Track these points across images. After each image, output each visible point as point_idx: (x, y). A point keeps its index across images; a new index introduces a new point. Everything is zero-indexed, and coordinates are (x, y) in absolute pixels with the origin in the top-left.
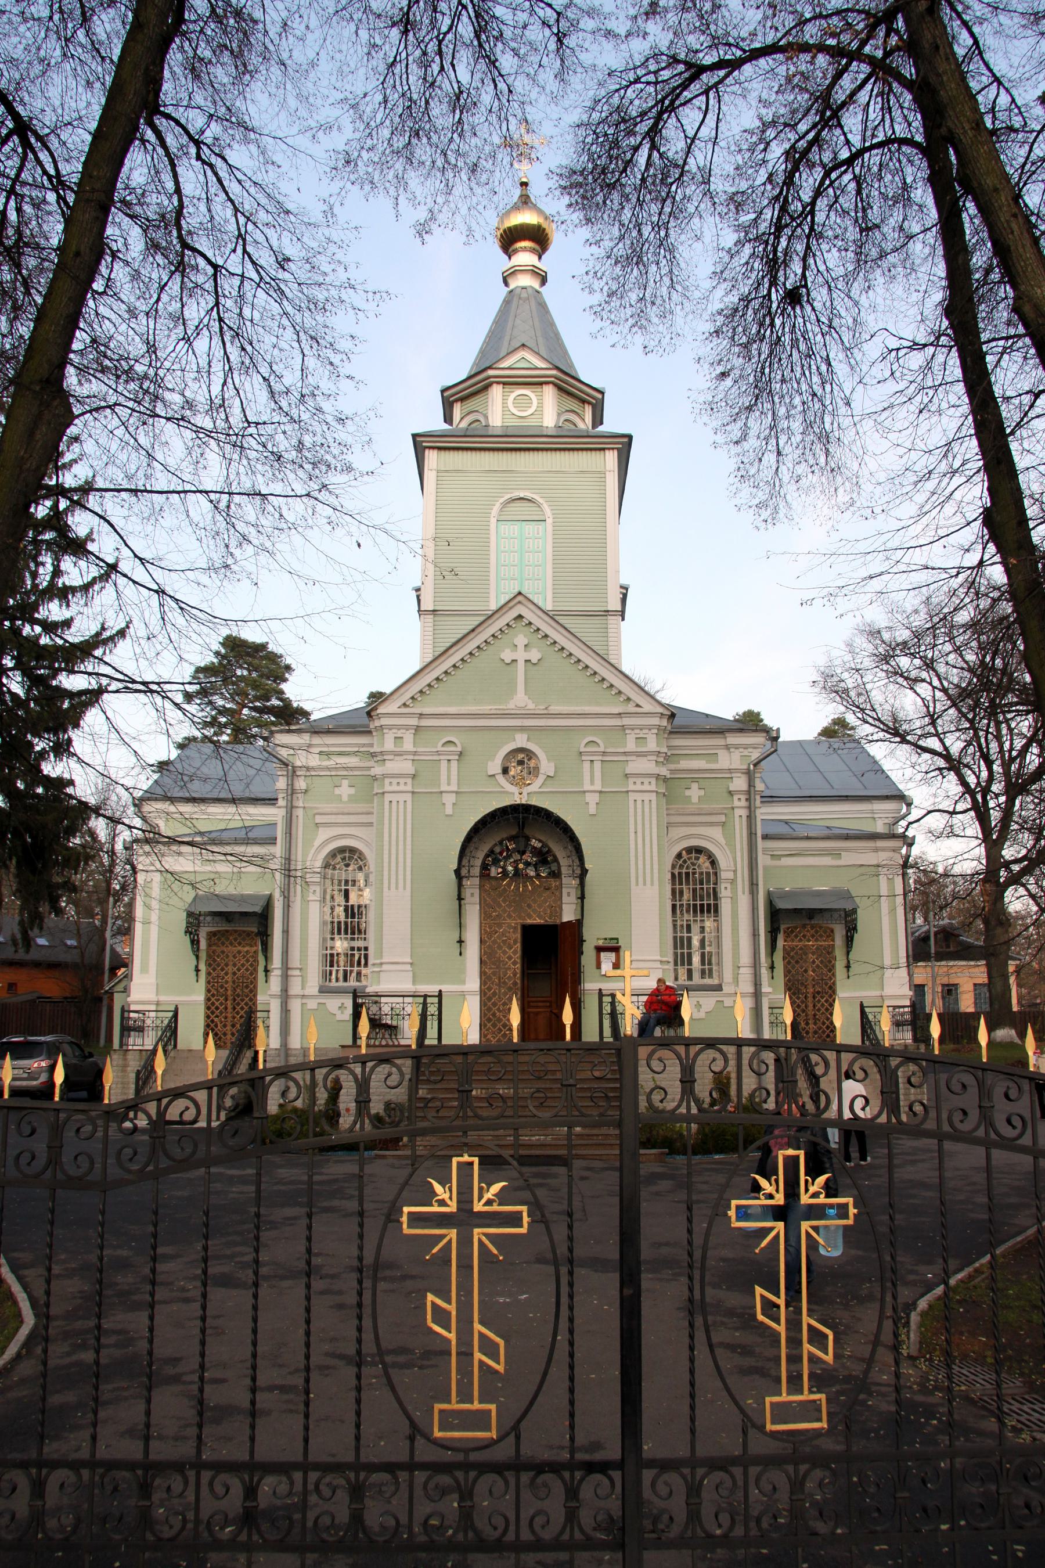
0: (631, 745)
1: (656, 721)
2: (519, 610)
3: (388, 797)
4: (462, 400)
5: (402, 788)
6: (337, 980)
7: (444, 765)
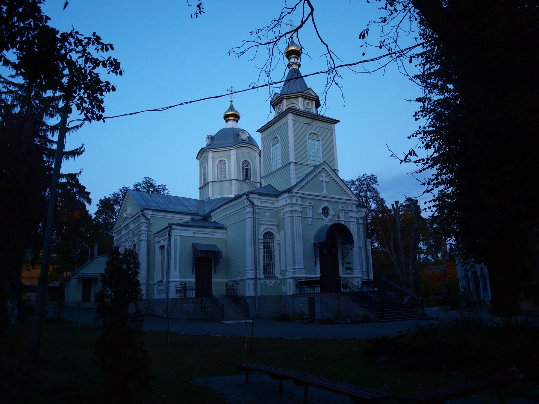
0: (350, 209)
1: (356, 202)
2: (324, 166)
3: (295, 218)
4: (287, 99)
5: (298, 215)
6: (269, 274)
7: (308, 209)
